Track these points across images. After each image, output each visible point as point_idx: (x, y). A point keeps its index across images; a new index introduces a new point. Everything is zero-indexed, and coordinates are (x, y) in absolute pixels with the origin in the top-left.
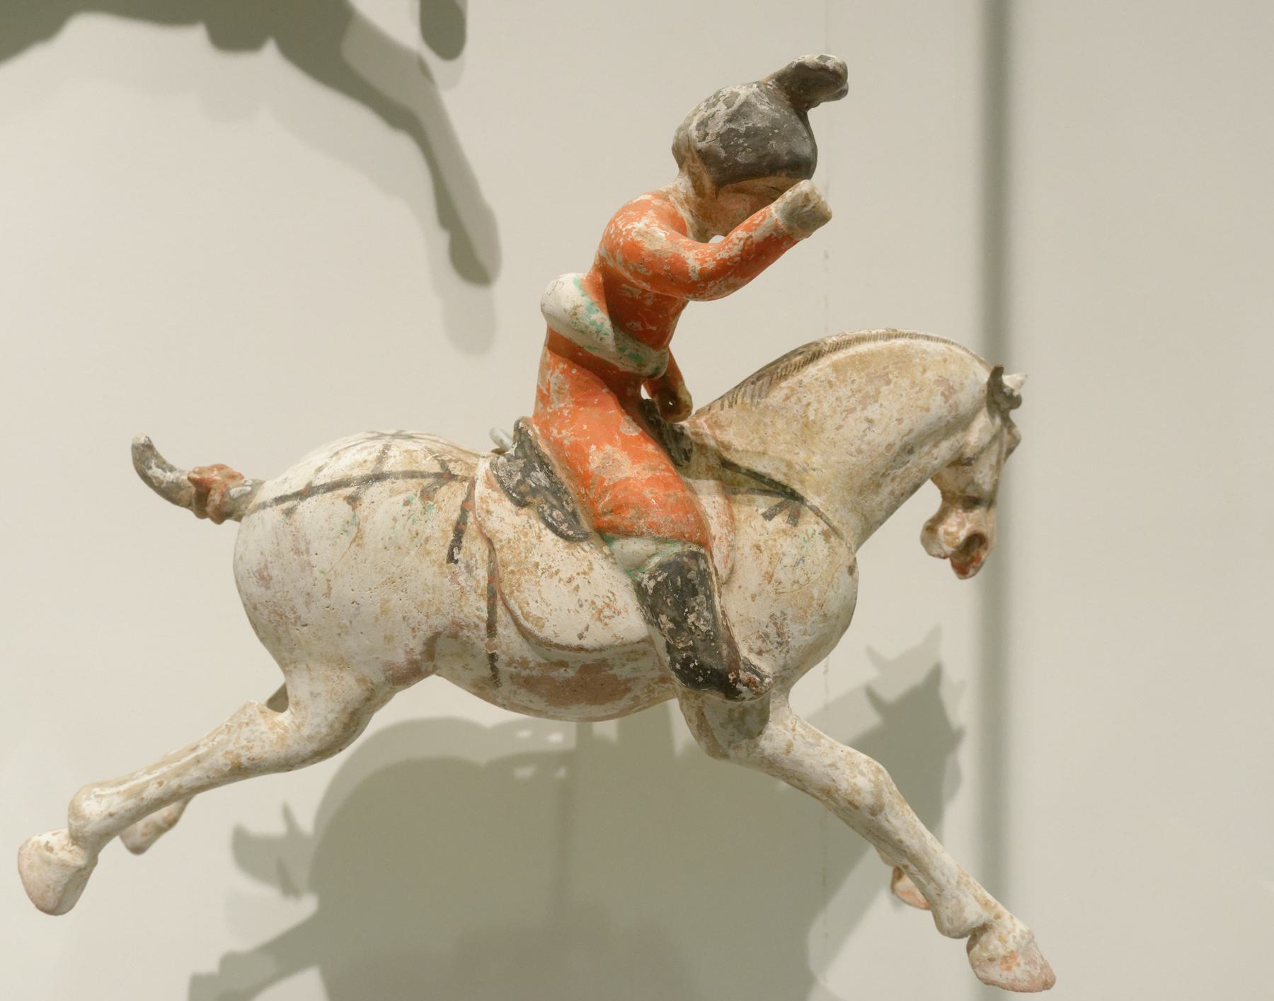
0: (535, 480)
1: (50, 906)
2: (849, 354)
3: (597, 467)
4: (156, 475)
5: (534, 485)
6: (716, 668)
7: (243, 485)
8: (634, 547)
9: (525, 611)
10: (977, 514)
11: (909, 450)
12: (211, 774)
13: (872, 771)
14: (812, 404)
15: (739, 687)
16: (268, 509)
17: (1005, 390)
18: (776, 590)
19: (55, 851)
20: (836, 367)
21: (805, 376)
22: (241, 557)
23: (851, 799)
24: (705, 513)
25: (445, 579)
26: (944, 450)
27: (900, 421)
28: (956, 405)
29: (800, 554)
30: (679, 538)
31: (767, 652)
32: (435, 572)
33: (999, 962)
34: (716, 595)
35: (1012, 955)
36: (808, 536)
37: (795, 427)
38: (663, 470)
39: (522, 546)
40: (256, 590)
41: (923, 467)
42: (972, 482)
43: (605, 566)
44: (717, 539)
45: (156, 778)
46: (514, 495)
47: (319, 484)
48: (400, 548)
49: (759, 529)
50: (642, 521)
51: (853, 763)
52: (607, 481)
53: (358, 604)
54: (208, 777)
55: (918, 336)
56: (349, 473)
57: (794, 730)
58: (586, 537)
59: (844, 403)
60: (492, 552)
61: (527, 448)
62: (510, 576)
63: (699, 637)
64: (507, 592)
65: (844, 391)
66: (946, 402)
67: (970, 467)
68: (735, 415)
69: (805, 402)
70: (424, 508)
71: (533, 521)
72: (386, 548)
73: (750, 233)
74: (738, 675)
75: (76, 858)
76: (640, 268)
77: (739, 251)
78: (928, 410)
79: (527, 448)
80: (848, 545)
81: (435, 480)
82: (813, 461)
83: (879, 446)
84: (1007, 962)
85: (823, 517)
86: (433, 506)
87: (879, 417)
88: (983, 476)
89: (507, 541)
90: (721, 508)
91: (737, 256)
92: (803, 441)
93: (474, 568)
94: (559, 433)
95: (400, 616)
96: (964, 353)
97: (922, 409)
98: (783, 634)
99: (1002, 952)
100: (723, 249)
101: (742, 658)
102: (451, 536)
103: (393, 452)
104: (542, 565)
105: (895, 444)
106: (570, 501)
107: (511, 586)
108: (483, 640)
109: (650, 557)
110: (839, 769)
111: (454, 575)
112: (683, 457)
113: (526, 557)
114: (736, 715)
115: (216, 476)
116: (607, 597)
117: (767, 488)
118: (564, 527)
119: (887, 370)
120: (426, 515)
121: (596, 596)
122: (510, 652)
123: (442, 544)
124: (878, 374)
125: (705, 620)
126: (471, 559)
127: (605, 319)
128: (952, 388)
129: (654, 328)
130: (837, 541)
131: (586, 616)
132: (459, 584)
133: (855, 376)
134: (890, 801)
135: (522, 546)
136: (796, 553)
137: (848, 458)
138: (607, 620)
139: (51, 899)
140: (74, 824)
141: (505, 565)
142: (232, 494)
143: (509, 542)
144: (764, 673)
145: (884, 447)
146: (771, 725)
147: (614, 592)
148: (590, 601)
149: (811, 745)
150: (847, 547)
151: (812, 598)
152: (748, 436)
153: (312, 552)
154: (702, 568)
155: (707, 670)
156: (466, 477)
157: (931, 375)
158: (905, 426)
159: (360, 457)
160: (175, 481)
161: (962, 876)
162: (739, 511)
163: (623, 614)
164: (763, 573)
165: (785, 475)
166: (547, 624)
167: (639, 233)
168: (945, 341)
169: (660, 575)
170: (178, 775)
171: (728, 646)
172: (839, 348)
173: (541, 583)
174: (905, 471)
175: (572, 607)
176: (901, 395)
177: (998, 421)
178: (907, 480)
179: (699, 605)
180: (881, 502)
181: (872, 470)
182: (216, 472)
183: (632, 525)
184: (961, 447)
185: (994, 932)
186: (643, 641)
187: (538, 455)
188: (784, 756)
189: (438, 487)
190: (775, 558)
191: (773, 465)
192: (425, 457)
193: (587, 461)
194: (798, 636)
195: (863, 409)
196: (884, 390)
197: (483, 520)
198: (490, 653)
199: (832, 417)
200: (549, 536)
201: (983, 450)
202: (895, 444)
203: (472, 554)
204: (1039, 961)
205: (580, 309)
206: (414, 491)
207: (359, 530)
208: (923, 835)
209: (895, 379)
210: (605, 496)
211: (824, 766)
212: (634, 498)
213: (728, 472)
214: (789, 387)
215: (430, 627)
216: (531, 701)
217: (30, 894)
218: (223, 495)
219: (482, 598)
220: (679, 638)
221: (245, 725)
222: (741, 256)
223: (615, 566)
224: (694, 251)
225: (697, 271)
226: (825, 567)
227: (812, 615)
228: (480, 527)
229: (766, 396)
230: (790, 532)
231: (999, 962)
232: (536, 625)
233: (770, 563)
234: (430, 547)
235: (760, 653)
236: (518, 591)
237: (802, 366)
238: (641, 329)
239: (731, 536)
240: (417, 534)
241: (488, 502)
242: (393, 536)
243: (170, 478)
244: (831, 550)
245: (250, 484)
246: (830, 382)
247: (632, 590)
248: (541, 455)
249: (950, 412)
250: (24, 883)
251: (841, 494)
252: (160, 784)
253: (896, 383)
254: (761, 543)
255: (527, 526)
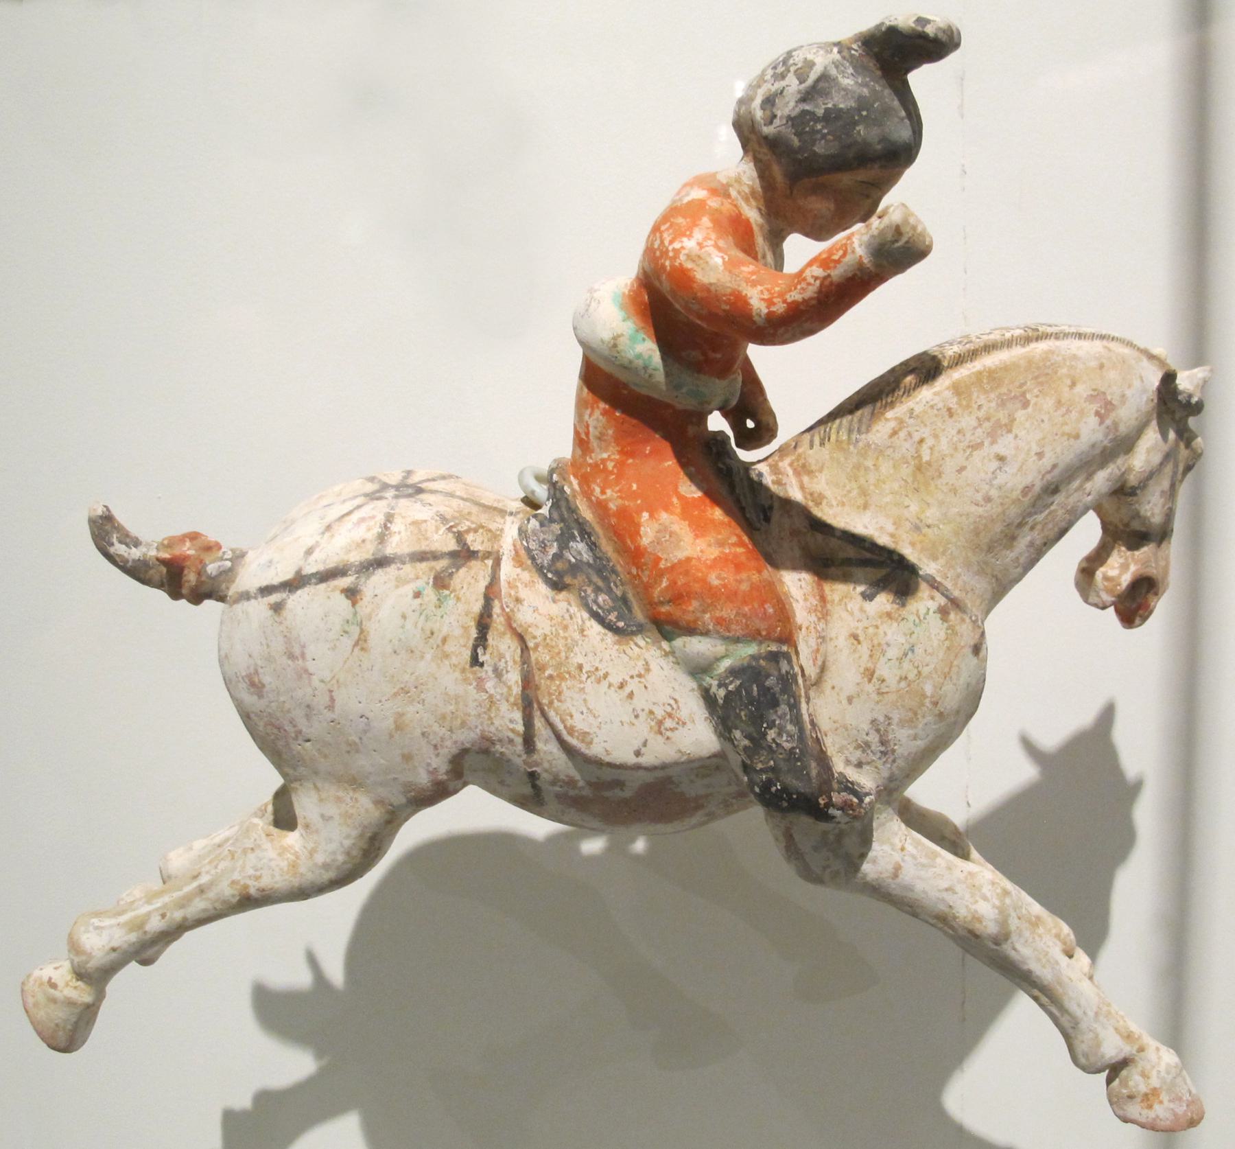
0: (575, 553)
1: (63, 1045)
2: (974, 370)
3: (651, 542)
4: (119, 553)
5: (573, 560)
6: (803, 791)
7: (222, 559)
8: (698, 646)
9: (568, 726)
10: (1145, 552)
11: (1052, 489)
12: (218, 906)
13: (998, 895)
14: (927, 441)
15: (832, 811)
16: (253, 601)
17: (1180, 398)
18: (878, 689)
19: (59, 988)
20: (957, 389)
21: (917, 403)
22: (226, 656)
23: (970, 927)
24: (788, 595)
25: (470, 687)
26: (1101, 480)
27: (1040, 455)
28: (1116, 425)
29: (909, 643)
30: (754, 636)
31: (868, 763)
32: (456, 679)
33: (1139, 1099)
34: (803, 700)
35: (1155, 1092)
36: (919, 618)
37: (906, 471)
38: (734, 545)
39: (561, 643)
40: (249, 699)
41: (1072, 507)
42: (1137, 515)
43: (665, 666)
44: (803, 629)
45: (157, 909)
46: (550, 575)
47: (310, 572)
48: (412, 652)
49: (857, 613)
50: (707, 616)
51: (974, 886)
52: (663, 562)
53: (368, 719)
54: (215, 909)
55: (1066, 335)
56: (346, 558)
57: (903, 849)
58: (640, 630)
59: (968, 435)
60: (525, 652)
61: (564, 509)
62: (548, 682)
63: (781, 756)
64: (545, 701)
65: (968, 421)
66: (1101, 423)
67: (1135, 498)
68: (827, 457)
69: (917, 437)
70: (439, 599)
71: (574, 609)
72: (395, 652)
73: (829, 271)
74: (830, 798)
75: (82, 994)
76: (693, 304)
77: (815, 293)
78: (1077, 437)
79: (564, 509)
80: (973, 618)
81: (451, 561)
82: (928, 514)
83: (1012, 491)
84: (1148, 1100)
85: (940, 588)
86: (450, 595)
87: (1013, 452)
88: (1152, 507)
89: (542, 638)
90: (809, 588)
91: (811, 299)
92: (915, 489)
93: (504, 672)
94: (603, 492)
95: (418, 732)
96: (1126, 351)
97: (1069, 436)
98: (888, 741)
99: (1143, 1088)
100: (795, 288)
101: (836, 775)
102: (474, 633)
103: (397, 526)
104: (586, 668)
105: (1033, 485)
106: (618, 583)
107: (550, 694)
108: (519, 756)
109: (718, 659)
110: (956, 893)
111: (480, 682)
112: (762, 517)
113: (567, 658)
114: (831, 837)
115: (188, 549)
116: (669, 704)
117: (868, 555)
118: (612, 617)
119: (1025, 387)
120: (441, 609)
121: (654, 704)
122: (554, 770)
123: (463, 644)
124: (1013, 394)
125: (790, 736)
126: (500, 660)
127: (654, 351)
128: (1110, 403)
129: (718, 356)
130: (958, 617)
131: (643, 729)
132: (487, 692)
133: (982, 400)
134: (1018, 928)
135: (561, 643)
136: (904, 642)
137: (974, 508)
138: (669, 734)
139: (62, 1038)
140: (77, 959)
141: (542, 668)
142: (209, 572)
143: (545, 639)
144: (864, 790)
145: (1019, 492)
146: (875, 846)
147: (677, 697)
148: (647, 710)
149: (923, 866)
150: (972, 621)
151: (924, 696)
152: (845, 486)
153: (309, 656)
154: (783, 671)
155: (792, 794)
156: (488, 552)
157: (1082, 390)
158: (1047, 462)
159: (361, 533)
160: (142, 559)
161: (1101, 1006)
162: (832, 591)
163: (689, 725)
164: (862, 670)
165: (892, 536)
166: (596, 740)
167: (689, 256)
168: (1102, 337)
169: (731, 682)
170: (182, 906)
171: (818, 765)
172: (962, 362)
173: (586, 690)
174: (1047, 516)
175: (626, 719)
176: (1043, 421)
177: (1172, 435)
178: (1050, 526)
179: (780, 718)
180: (1017, 558)
181: (1004, 521)
182: (188, 544)
183: (695, 621)
184: (1124, 473)
185: (1136, 1067)
186: (715, 756)
187: (577, 521)
188: (890, 880)
189: (454, 570)
190: (877, 650)
191: (877, 523)
192: (437, 529)
193: (638, 533)
194: (905, 741)
195: (993, 442)
196: (1020, 415)
197: (512, 610)
198: (530, 770)
199: (952, 456)
200: (595, 628)
201: (1151, 475)
202: (1033, 485)
203: (500, 654)
204: (1187, 1097)
205: (621, 339)
206: (426, 579)
207: (362, 631)
208: (1057, 963)
209: (1035, 399)
210: (662, 581)
211: (939, 891)
212: (697, 585)
213: (819, 537)
214: (896, 419)
215: (456, 742)
216: (583, 821)
217: (40, 1034)
218: (199, 574)
219: (515, 708)
220: (756, 757)
221: (249, 851)
222: (818, 299)
223: (676, 666)
224: (759, 288)
225: (763, 316)
226: (941, 655)
227: (924, 717)
228: (509, 620)
229: (868, 431)
230: (897, 615)
231: (1139, 1099)
232: (583, 741)
233: (871, 656)
234: (450, 647)
235: (859, 765)
236: (560, 701)
237: (914, 389)
238: (701, 358)
239: (821, 626)
240: (432, 633)
241: (517, 587)
242: (402, 637)
243: (135, 554)
244: (949, 631)
245: (229, 557)
246: (949, 410)
247: (699, 696)
248: (581, 520)
249: (1106, 435)
250: (32, 1023)
251: (964, 554)
252: (163, 916)
253: (1036, 404)
254: (859, 632)
255: (567, 616)
